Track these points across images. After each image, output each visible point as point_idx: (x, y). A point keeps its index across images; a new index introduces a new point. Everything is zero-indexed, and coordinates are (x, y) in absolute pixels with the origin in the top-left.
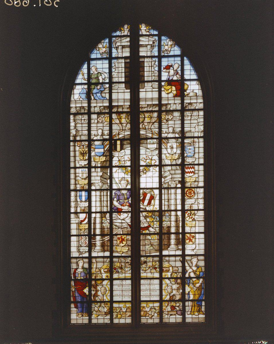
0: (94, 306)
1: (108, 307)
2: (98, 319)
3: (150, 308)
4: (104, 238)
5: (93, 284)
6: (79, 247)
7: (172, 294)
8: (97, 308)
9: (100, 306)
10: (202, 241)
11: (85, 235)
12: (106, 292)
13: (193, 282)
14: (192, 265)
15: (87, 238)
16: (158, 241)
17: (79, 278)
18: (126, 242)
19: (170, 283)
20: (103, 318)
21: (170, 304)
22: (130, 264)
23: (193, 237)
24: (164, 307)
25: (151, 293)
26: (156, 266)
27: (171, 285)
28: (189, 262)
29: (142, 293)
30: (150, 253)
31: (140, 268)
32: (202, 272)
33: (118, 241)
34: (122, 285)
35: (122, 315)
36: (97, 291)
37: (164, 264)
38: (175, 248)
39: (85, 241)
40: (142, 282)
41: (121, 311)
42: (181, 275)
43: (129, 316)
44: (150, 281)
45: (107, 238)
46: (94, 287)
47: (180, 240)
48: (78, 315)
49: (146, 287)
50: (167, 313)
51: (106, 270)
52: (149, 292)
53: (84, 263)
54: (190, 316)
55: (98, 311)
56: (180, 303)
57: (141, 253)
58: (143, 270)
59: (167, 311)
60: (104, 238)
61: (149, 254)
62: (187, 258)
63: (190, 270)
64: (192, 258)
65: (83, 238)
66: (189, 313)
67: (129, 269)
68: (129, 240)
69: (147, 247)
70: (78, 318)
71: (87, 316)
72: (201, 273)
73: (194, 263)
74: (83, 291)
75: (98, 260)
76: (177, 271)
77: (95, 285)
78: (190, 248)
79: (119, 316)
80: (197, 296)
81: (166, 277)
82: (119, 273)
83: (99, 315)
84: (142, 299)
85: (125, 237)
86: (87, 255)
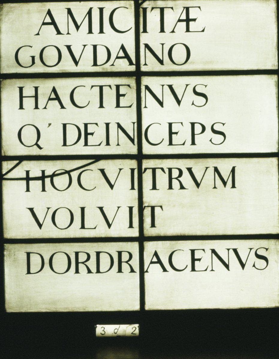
25: (149, 197)
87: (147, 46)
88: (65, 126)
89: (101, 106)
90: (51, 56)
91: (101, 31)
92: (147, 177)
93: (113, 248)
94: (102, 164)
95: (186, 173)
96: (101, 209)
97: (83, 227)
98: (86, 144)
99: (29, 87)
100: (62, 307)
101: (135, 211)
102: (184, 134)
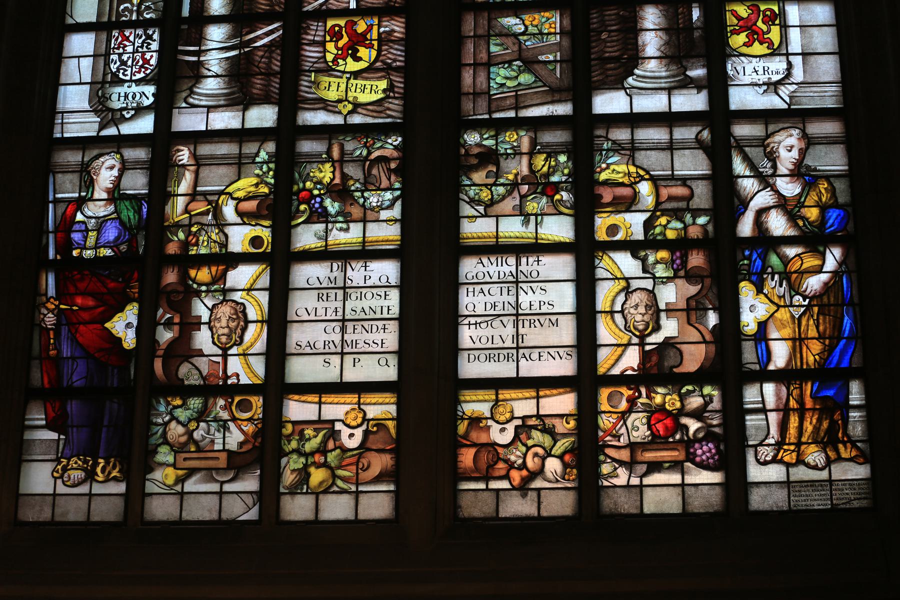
0: (167, 418)
1: (250, 420)
2: (182, 494)
3: (519, 422)
4: (252, 36)
5: (169, 289)
6: (104, 82)
7: (657, 338)
8: (181, 430)
9: (201, 416)
10: (825, 40)
11: (146, 24)
12: (244, 329)
13: (786, 266)
14: (775, 167)
15: (156, 36)
16: (566, 43)
17: (88, 254)
18: (374, 53)
19: (645, 270)
20: (215, 487)
21: (643, 400)
22: (395, 171)
23: (771, 19)
24: (605, 421)
25: (521, 331)
26: (555, 179)
27: (648, 284)
28: (754, 153)
29: (467, 335)
30: (517, 108)
31: (458, 188)
32: (836, 205)
33: (330, 46)
34: (344, 288)
35: (340, 472)
36: (190, 325)
37: (604, 166)
38: (664, 74)
39: (143, 54)
40: (469, 267)
41: (331, 445)
42: (710, 228)
43: (377, 480)
44: (518, 264)
45: (267, 34)
46: (173, 307)
47: (697, 34)
48: (65, 469)
49: (490, 299)
50: (625, 455)
51: (251, 205)
52: (510, 330)
53: (122, 171)
54: (775, 473)
55: (186, 444)
56: (707, 390)
57: (467, 105)
58: (472, 202)
59: (623, 441)
60: (252, 36)
61: (511, 114)
62: (742, 130)
63: (764, 199)
64: (771, 128)
65: (132, 38)
66: (766, 453)
67: (388, 196)
68: (392, 41)
69: (500, 74)
70: (61, 489)
71: (115, 479)
72: (833, 215)
73: (787, 158)
74: (108, 325)
75: (205, 149)
76: (682, 205)
77: (181, 288)
78: (755, 78)
79: (317, 476)
80: (816, 347)
81: (619, 237)
82: (327, 222)
83: (191, 472)
84: (469, 369)
85: (370, 28)
86: (145, 125)
87: (521, 271)
88: (486, 303)
89: (501, 295)
90: (481, 275)
91: (502, 266)
92: (520, 323)
93: (505, 352)
94: (501, 318)
95: (537, 321)
96: (500, 336)
97: (493, 343)
98: (495, 310)
99: (471, 288)
100: (483, 376)
101: (515, 337)
102: (536, 305)
